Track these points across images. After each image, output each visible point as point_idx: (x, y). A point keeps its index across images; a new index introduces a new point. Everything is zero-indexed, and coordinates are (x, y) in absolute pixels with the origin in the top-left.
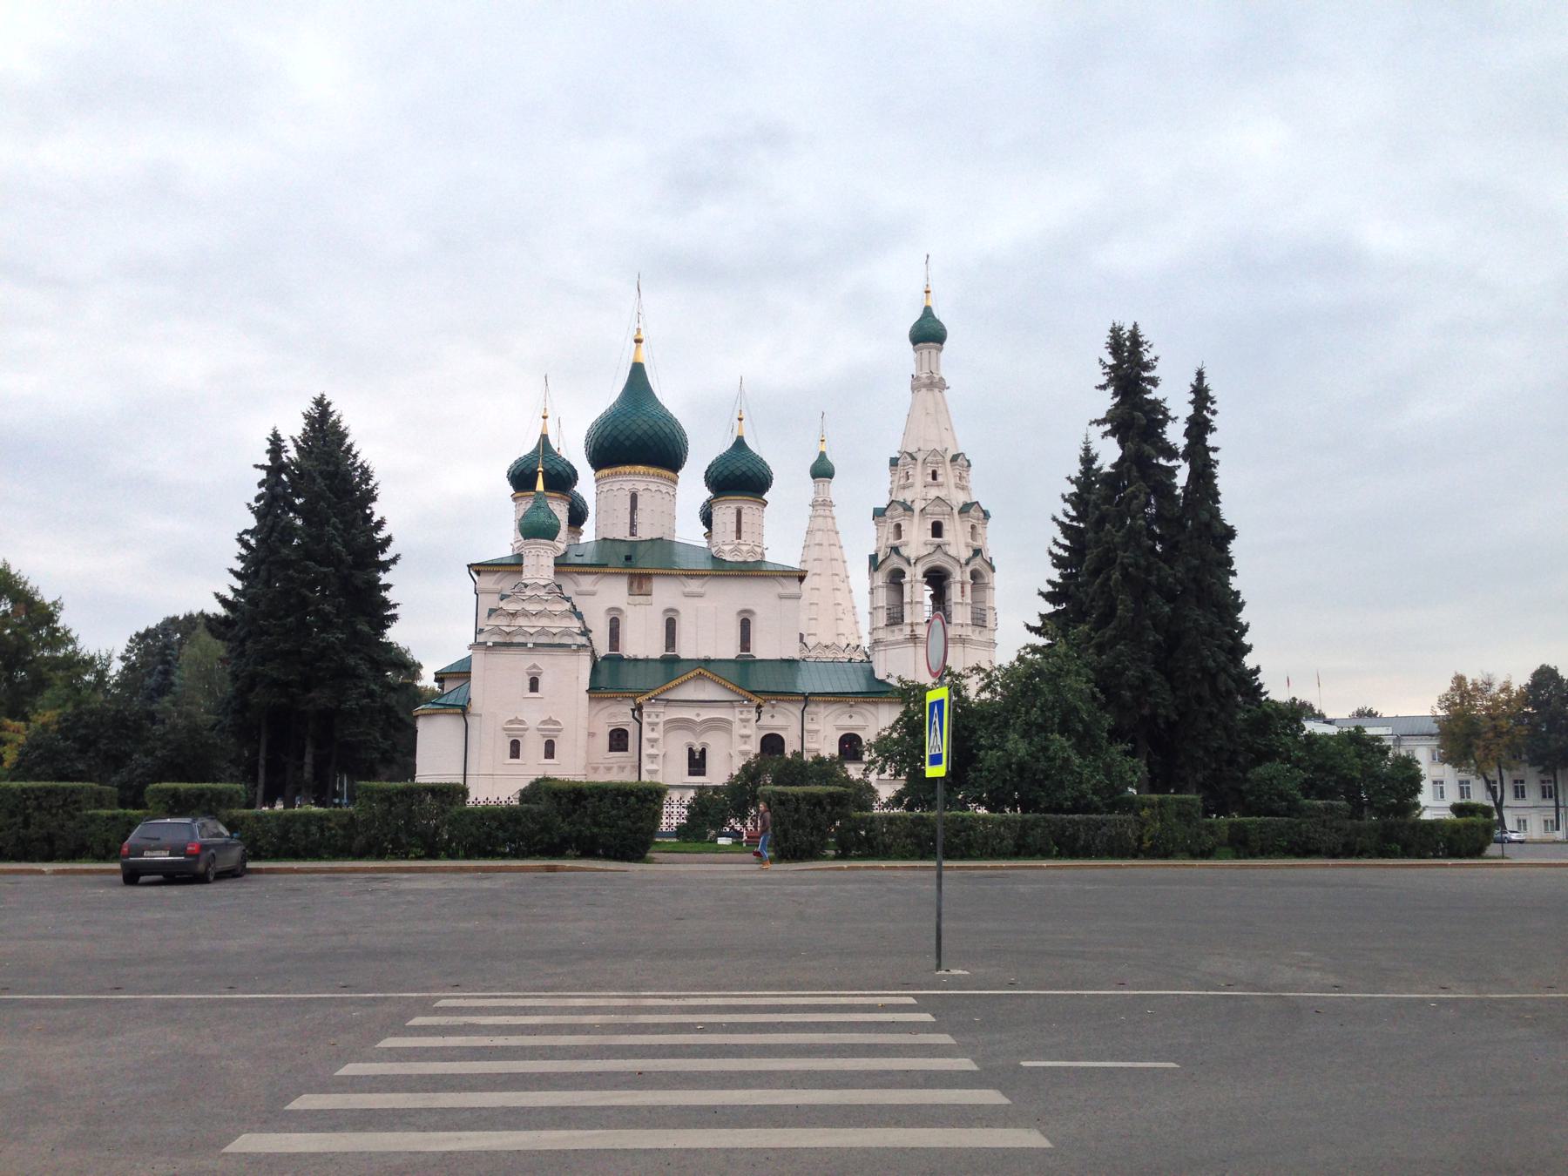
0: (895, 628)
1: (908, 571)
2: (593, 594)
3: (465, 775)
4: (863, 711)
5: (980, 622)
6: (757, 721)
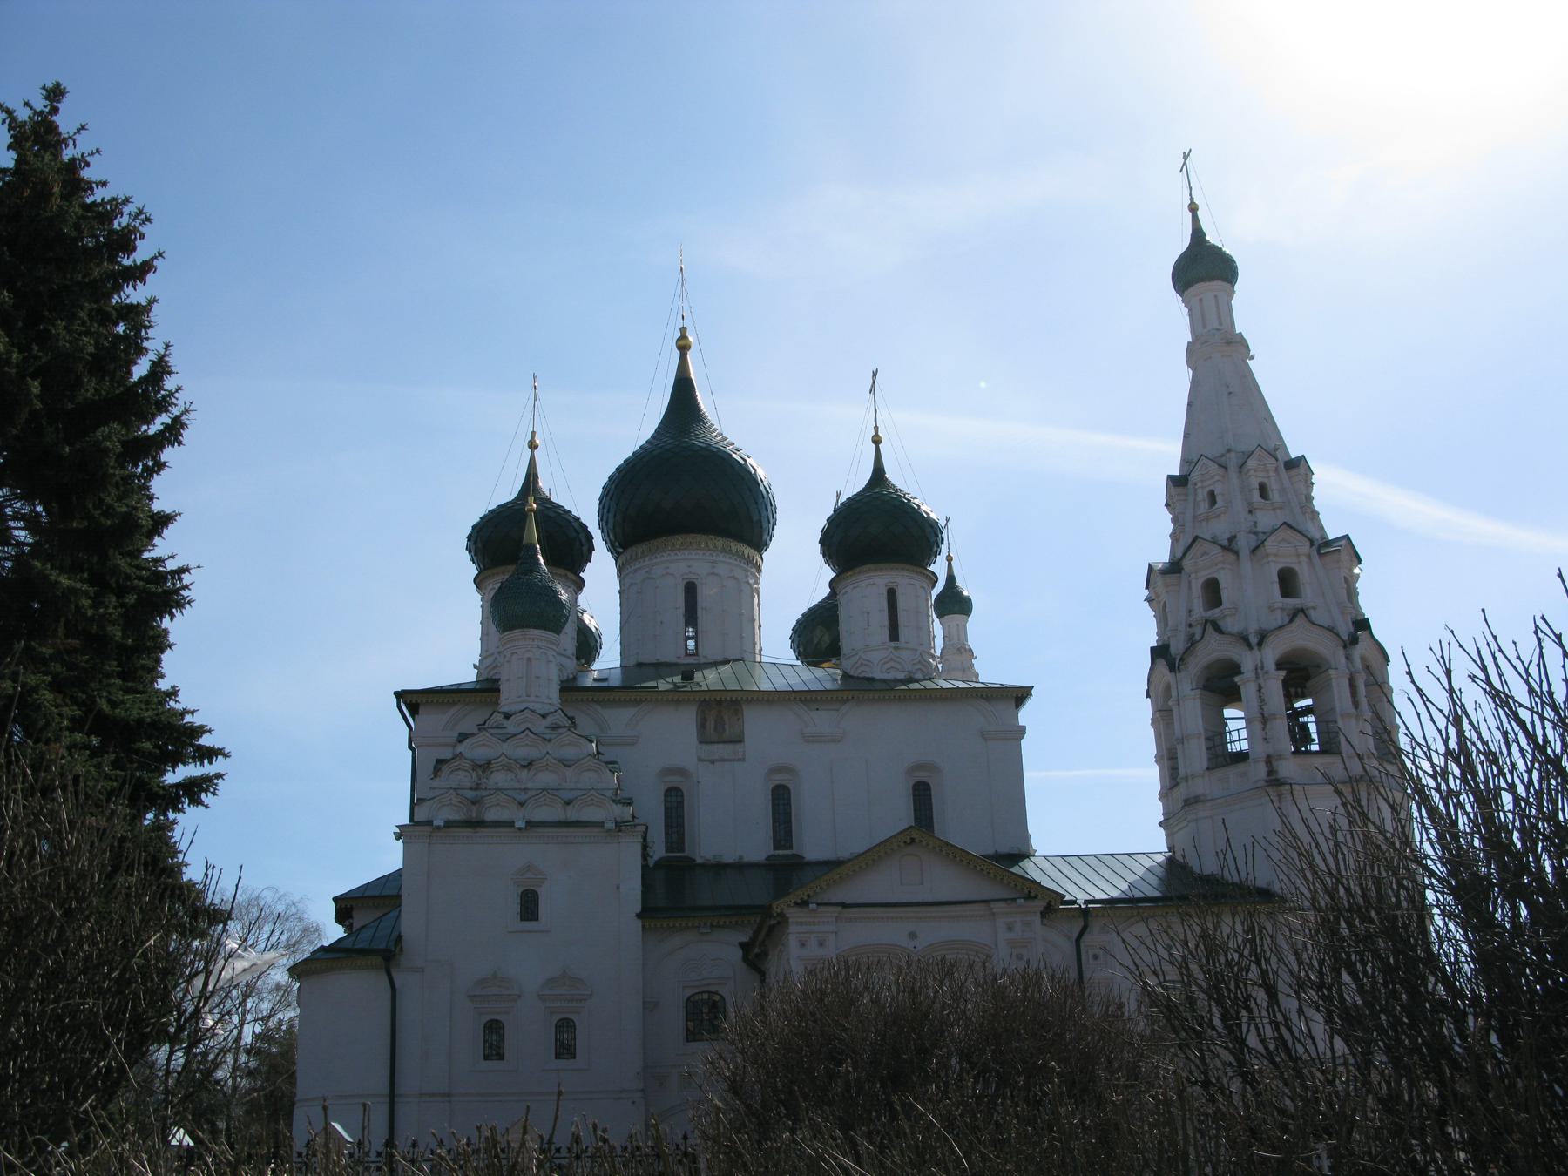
1: (1248, 660)
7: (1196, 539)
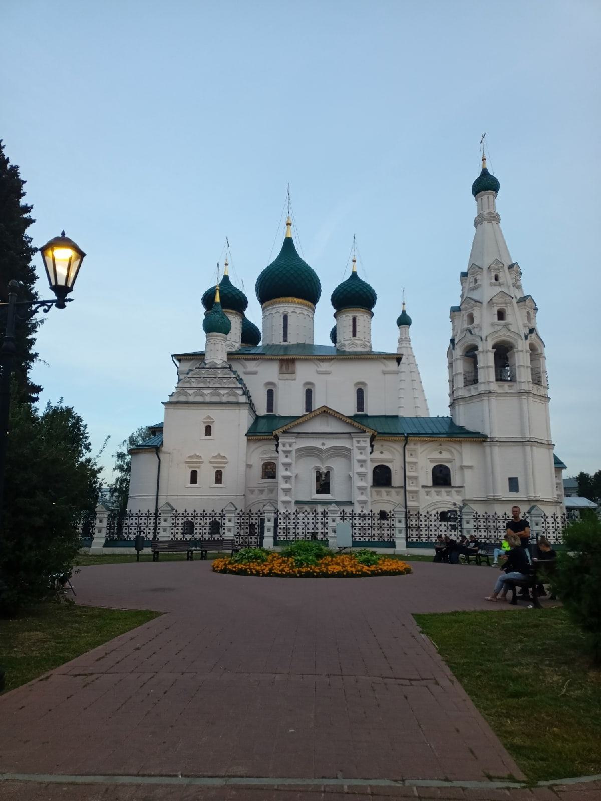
0: (472, 388)
2: (255, 373)
3: (157, 495)
4: (451, 448)
5: (537, 382)
6: (371, 453)
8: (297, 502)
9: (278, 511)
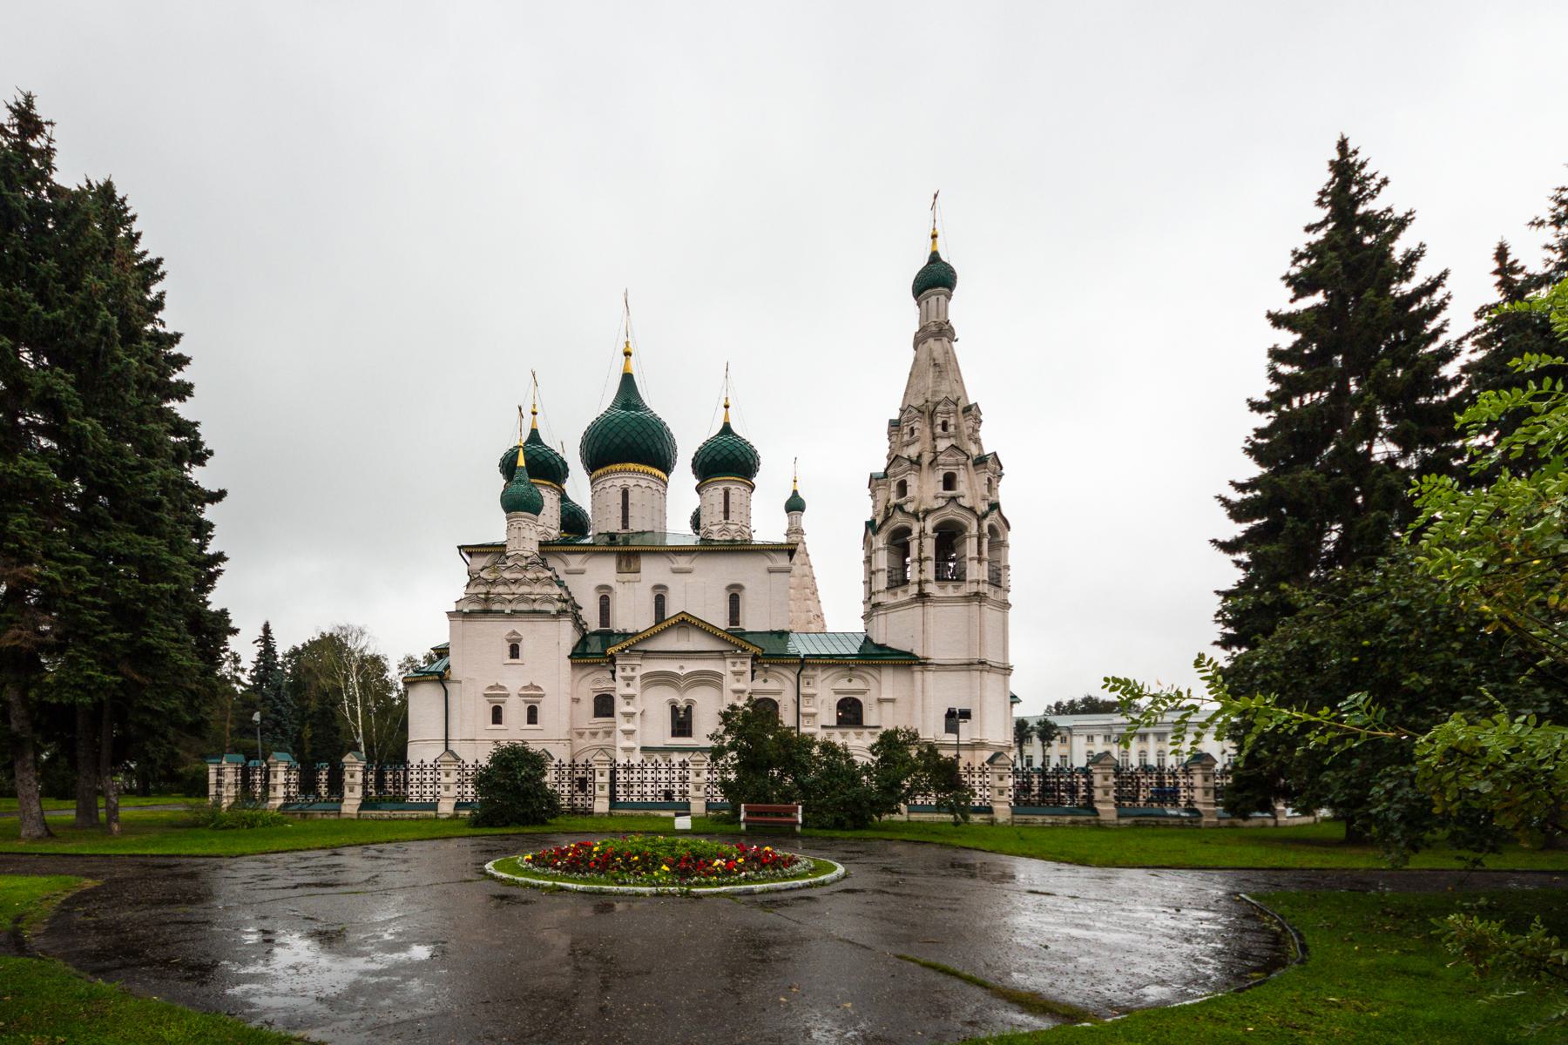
0: (899, 591)
3: (447, 740)
7: (897, 456)
8: (644, 749)
9: (615, 761)
